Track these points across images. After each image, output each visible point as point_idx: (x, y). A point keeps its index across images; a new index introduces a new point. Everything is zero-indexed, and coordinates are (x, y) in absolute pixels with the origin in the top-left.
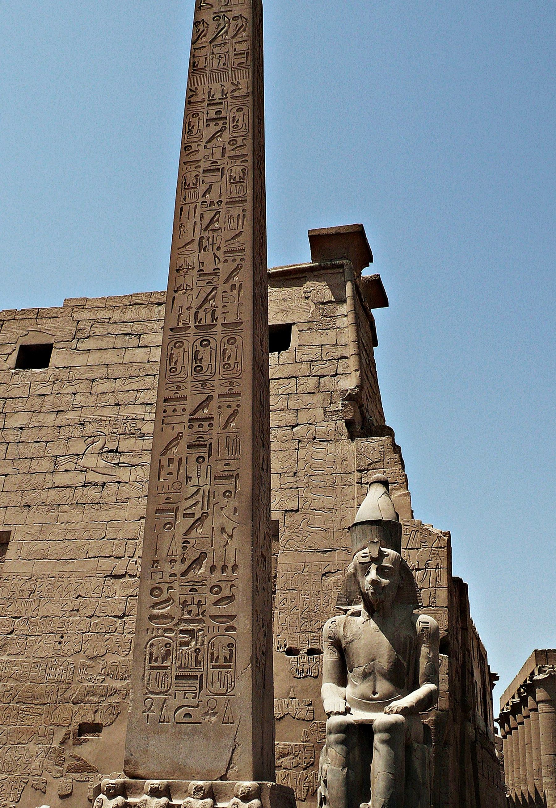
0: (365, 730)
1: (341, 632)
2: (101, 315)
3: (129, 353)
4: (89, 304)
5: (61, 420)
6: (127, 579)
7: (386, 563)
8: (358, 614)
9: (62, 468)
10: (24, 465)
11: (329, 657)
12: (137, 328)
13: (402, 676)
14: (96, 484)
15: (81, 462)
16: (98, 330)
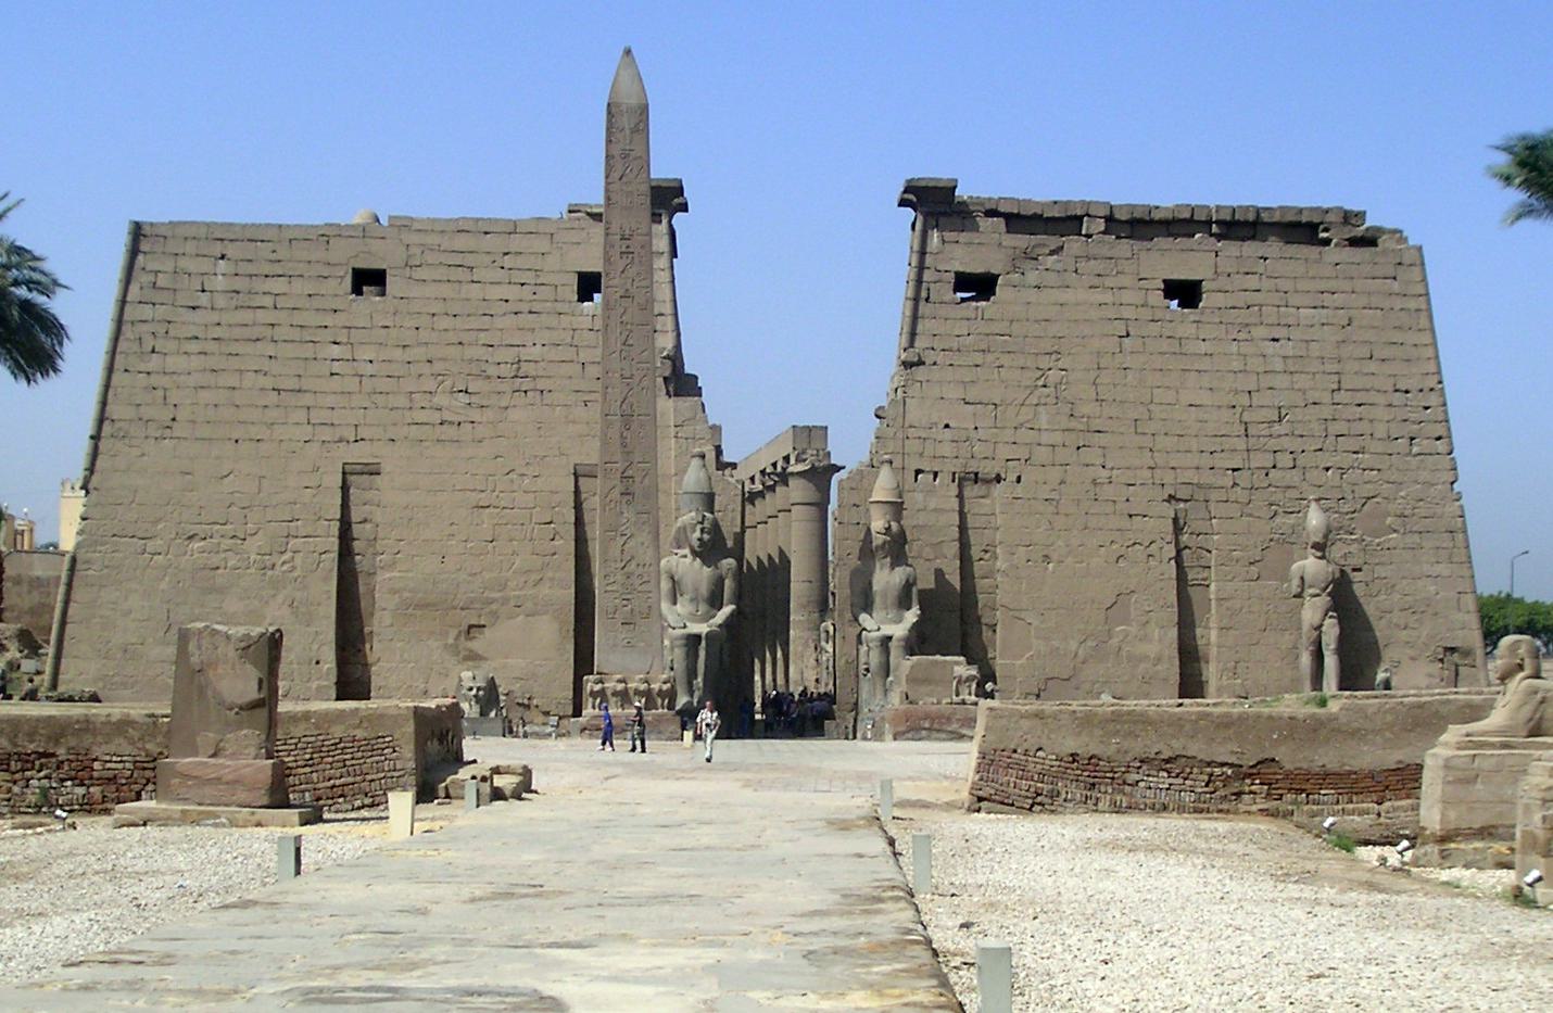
0: (696, 638)
1: (674, 569)
2: (431, 240)
3: (465, 287)
4: (417, 226)
5: (411, 354)
6: (491, 510)
7: (706, 524)
8: (685, 556)
9: (419, 405)
10: (380, 399)
11: (665, 585)
12: (469, 260)
13: (715, 601)
14: (451, 423)
15: (436, 400)
16: (430, 258)
